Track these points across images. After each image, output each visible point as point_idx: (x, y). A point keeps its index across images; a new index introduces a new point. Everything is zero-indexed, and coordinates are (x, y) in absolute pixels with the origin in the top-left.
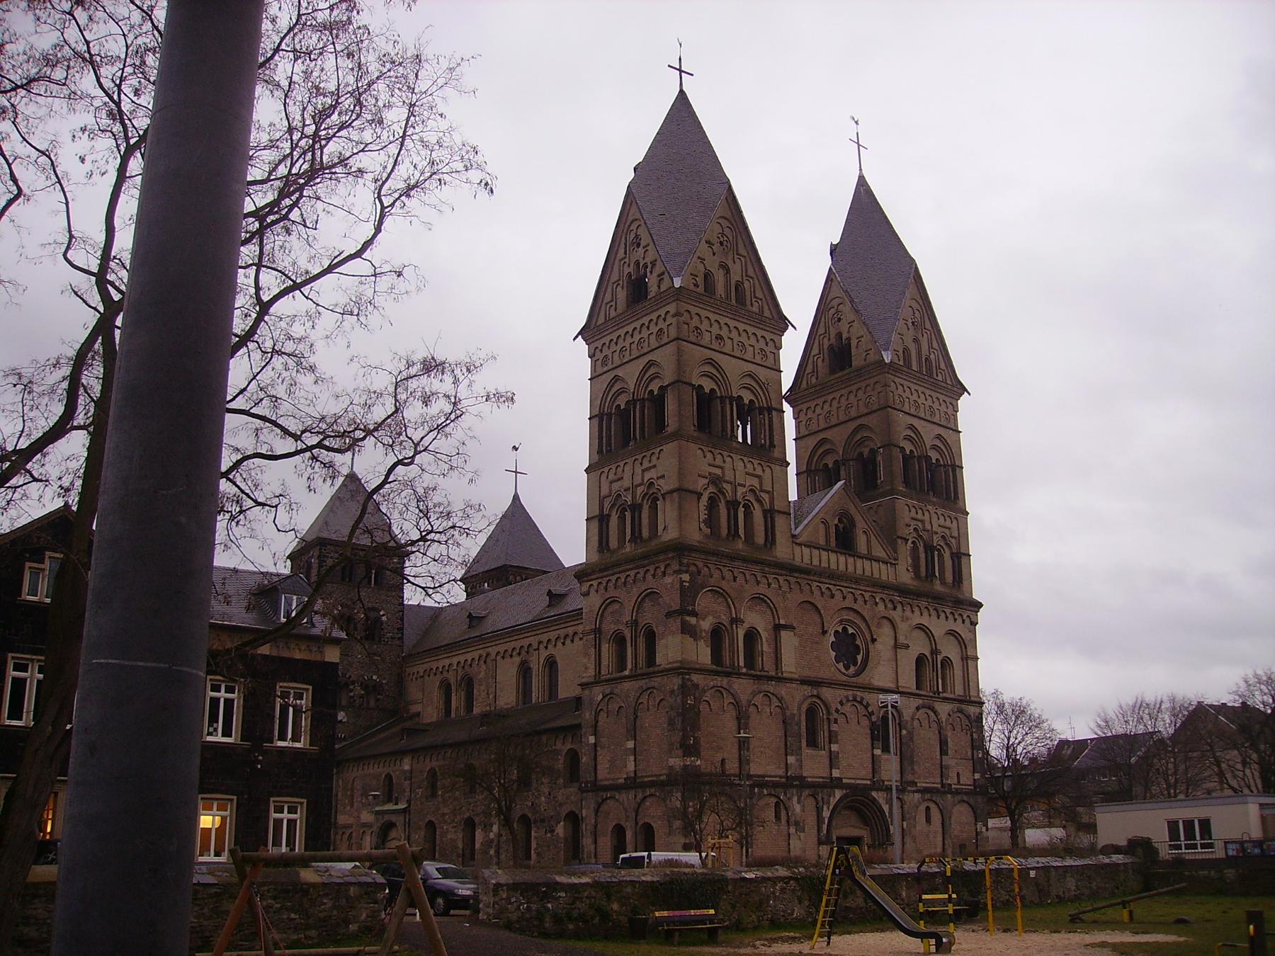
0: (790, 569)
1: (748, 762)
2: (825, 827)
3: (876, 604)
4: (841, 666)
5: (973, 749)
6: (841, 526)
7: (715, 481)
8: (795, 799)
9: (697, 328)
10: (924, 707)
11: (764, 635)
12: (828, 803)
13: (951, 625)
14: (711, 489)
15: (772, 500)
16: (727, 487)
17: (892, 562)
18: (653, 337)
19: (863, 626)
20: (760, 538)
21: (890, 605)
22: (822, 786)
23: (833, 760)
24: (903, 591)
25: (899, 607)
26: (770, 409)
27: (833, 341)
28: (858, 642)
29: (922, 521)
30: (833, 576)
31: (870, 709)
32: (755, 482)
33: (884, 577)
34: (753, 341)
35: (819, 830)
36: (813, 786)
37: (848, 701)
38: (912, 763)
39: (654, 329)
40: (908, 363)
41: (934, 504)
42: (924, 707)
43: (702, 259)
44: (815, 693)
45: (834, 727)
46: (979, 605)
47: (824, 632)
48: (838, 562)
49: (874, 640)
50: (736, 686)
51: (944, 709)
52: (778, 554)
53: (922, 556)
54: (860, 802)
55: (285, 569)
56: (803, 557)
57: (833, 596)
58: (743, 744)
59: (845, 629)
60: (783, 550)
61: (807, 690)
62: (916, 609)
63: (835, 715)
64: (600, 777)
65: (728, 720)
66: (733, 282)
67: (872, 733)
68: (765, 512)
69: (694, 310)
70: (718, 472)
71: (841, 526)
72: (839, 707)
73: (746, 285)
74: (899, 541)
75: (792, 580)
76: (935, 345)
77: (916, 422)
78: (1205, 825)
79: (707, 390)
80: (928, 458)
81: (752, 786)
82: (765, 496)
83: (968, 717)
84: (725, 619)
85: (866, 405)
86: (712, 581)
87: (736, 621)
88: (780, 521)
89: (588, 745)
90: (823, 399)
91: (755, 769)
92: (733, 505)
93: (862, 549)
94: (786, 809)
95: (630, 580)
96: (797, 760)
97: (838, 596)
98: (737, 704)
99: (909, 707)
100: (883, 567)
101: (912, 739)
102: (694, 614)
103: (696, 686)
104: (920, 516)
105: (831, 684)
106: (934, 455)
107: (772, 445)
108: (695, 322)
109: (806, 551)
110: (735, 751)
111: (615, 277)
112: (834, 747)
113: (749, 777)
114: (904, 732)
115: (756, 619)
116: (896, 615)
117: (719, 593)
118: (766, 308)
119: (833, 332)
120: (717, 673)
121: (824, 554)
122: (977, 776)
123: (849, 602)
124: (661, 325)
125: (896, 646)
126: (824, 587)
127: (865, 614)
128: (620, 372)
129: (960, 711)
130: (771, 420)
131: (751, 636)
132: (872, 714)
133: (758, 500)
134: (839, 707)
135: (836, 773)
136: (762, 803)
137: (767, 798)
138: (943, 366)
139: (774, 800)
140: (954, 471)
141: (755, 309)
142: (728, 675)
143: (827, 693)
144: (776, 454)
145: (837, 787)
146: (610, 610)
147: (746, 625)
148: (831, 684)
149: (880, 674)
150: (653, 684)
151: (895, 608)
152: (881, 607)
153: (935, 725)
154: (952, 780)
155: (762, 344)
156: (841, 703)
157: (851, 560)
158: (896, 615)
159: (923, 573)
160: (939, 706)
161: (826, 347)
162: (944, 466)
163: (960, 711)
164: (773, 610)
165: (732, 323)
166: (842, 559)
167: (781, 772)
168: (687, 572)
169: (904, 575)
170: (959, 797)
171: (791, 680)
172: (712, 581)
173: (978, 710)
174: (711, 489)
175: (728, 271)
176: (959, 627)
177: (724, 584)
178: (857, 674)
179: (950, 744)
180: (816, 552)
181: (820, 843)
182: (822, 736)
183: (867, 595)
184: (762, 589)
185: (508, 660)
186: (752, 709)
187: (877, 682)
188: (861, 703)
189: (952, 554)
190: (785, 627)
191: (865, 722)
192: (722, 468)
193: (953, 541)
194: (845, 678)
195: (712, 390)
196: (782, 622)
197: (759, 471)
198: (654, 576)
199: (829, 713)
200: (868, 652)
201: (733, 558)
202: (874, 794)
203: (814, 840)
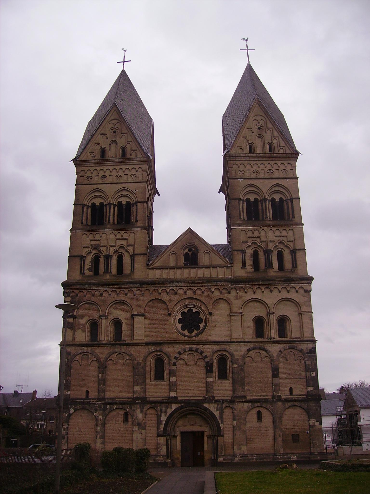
0: (141, 283)
1: (104, 391)
2: (162, 426)
3: (212, 292)
4: (186, 332)
5: (306, 370)
6: (190, 253)
7: (96, 247)
8: (138, 410)
9: (89, 177)
12: (166, 412)
13: (285, 294)
14: (94, 252)
16: (104, 249)
17: (230, 265)
19: (202, 307)
21: (224, 291)
22: (161, 402)
23: (172, 387)
24: (237, 282)
25: (233, 292)
28: (201, 316)
30: (173, 282)
31: (204, 355)
32: (124, 243)
34: (127, 172)
35: (158, 427)
36: (154, 404)
37: (185, 351)
38: (243, 384)
41: (269, 225)
42: (254, 349)
43: (98, 144)
44: (158, 349)
45: (174, 368)
46: (312, 279)
48: (186, 273)
50: (97, 351)
51: (274, 350)
52: (136, 277)
54: (192, 408)
57: (176, 293)
58: (102, 382)
59: (190, 310)
60: (139, 274)
61: (152, 348)
63: (174, 361)
65: (93, 369)
67: (207, 369)
69: (86, 169)
71: (190, 253)
72: (178, 356)
75: (144, 289)
76: (276, 134)
77: (253, 182)
81: (105, 404)
82: (131, 249)
83: (301, 351)
84: (96, 316)
86: (85, 298)
91: (108, 395)
92: (108, 257)
94: (132, 416)
96: (142, 388)
97: (180, 293)
98: (98, 360)
99: (238, 351)
101: (243, 370)
102: (74, 317)
103: (69, 354)
105: (170, 343)
108: (89, 173)
109: (158, 272)
110: (96, 386)
112: (173, 379)
113: (104, 399)
115: (121, 314)
117: (91, 304)
118: (139, 153)
122: (310, 389)
123: (190, 294)
125: (231, 315)
126: (168, 289)
127: (203, 299)
131: (117, 324)
132: (206, 357)
134: (178, 356)
135: (173, 394)
136: (112, 414)
137: (118, 411)
138: (282, 144)
139: (122, 412)
140: (292, 202)
143: (167, 349)
145: (173, 403)
147: (110, 318)
148: (170, 343)
151: (229, 292)
152: (217, 293)
153: (267, 360)
154: (284, 393)
155: (134, 172)
156: (180, 353)
158: (231, 296)
160: (269, 347)
162: (286, 201)
163: (294, 348)
164: (130, 307)
165: (111, 168)
167: (130, 396)
168: (69, 296)
169: (239, 272)
170: (290, 404)
171: (138, 344)
172: (85, 298)
173: (310, 346)
174: (94, 252)
176: (292, 295)
177: (93, 299)
179: (282, 369)
181: (159, 435)
182: (166, 373)
184: (122, 297)
187: (213, 338)
188: (196, 351)
189: (291, 251)
190: (137, 315)
191: (202, 363)
193: (291, 244)
196: (135, 313)
197: (125, 236)
199: (169, 360)
201: (106, 284)
202: (206, 405)
203: (155, 434)
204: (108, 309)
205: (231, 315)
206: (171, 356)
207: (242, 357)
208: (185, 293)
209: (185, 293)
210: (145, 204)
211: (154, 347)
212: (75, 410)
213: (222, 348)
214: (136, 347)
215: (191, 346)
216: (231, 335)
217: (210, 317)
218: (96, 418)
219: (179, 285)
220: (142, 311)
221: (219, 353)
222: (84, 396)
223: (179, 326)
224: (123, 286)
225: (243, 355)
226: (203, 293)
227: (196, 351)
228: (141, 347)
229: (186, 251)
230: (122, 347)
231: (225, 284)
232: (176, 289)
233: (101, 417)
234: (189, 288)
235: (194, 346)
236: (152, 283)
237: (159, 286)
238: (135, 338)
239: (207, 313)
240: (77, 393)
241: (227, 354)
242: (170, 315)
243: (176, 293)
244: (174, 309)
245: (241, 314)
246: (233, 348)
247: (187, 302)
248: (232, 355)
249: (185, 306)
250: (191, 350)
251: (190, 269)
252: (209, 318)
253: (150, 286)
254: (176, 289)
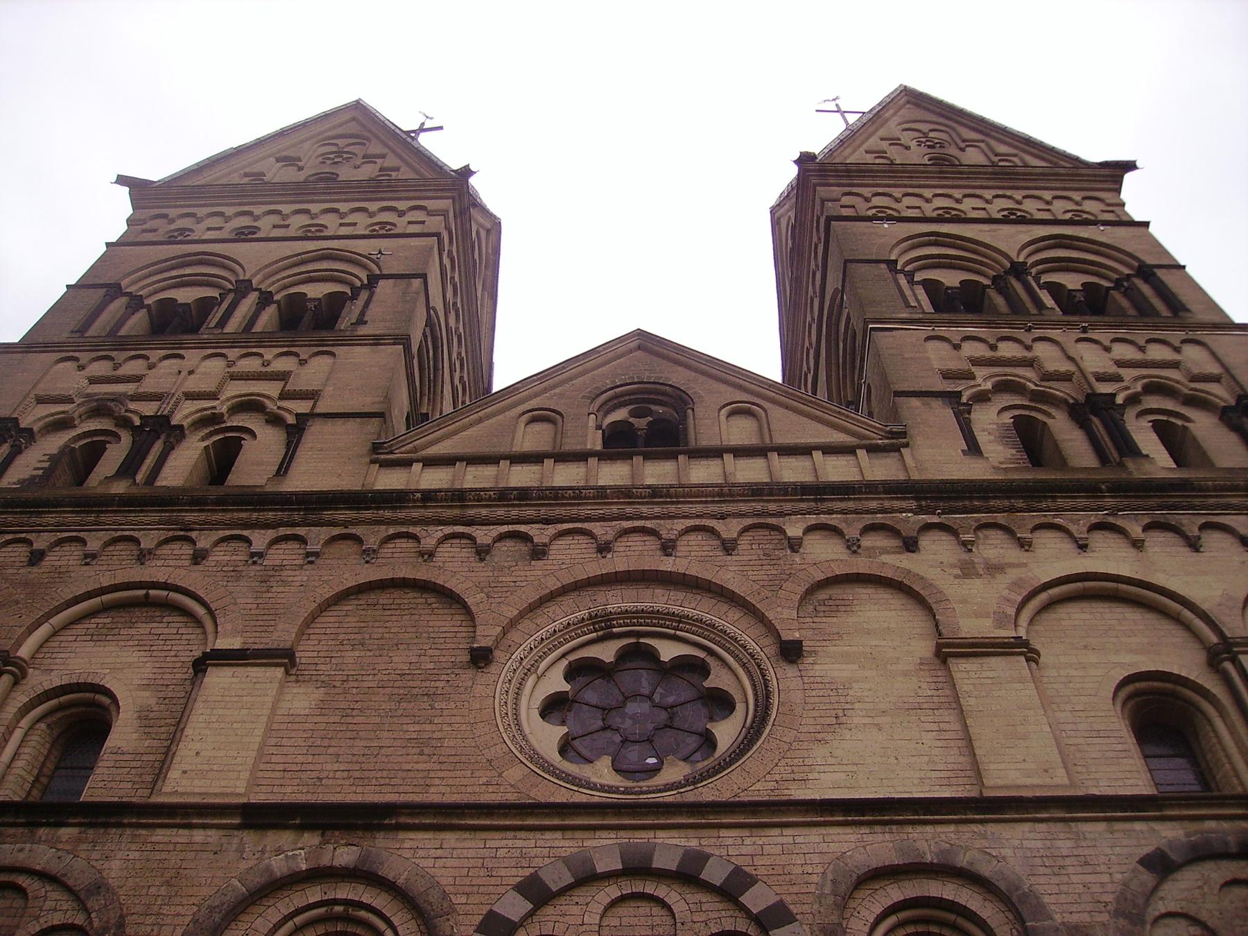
3: (795, 545)
24: (944, 499)
28: (718, 679)
37: (587, 878)
44: (344, 855)
49: (791, 652)
61: (291, 851)
126: (483, 535)
147: (39, 681)
188: (688, 875)
196: (222, 644)
197: (281, 365)
204: (45, 629)
205: (949, 650)
206: (452, 910)
207: (1117, 913)
209: (604, 548)
210: (417, 283)
211: (311, 839)
213: (922, 846)
214: (160, 835)
215: (642, 837)
217: (790, 671)
219: (560, 511)
220: (282, 635)
221: (895, 893)
223: (547, 737)
225: (1122, 897)
226: (729, 547)
227: (688, 875)
228: (199, 836)
229: (620, 415)
230: (42, 832)
231: (873, 504)
232: (541, 534)
234: (627, 524)
239: (762, 648)
242: (481, 658)
243: (539, 553)
244: (514, 636)
245: (1022, 648)
246: (1010, 848)
247: (616, 601)
249: (603, 626)
251: (637, 460)
252: (784, 679)
253: (367, 514)
254: (541, 534)
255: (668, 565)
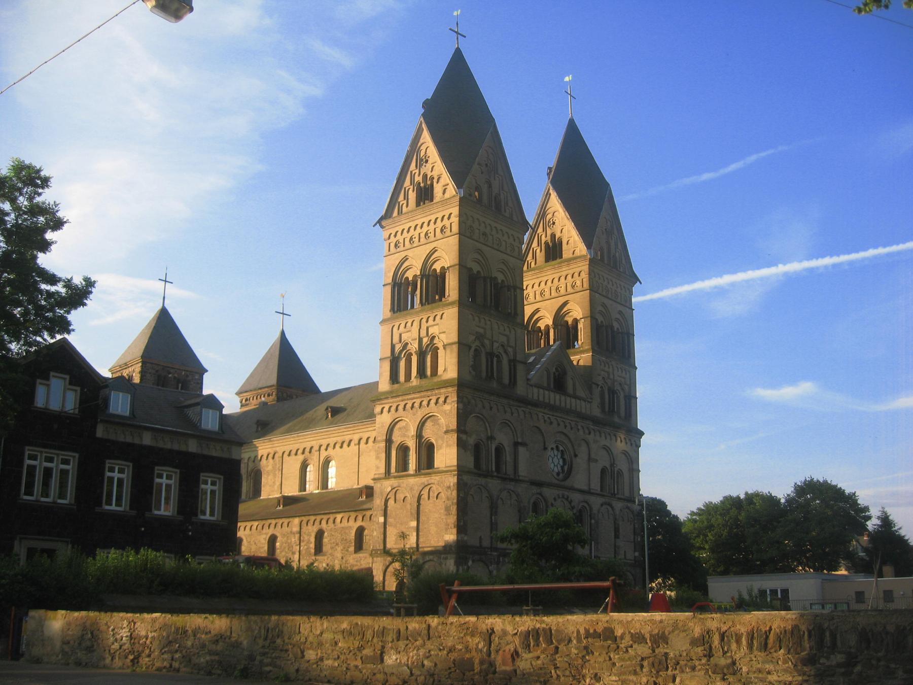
5: (635, 534)
9: (471, 227)
10: (605, 503)
11: (507, 449)
14: (477, 343)
15: (515, 353)
16: (487, 342)
18: (438, 231)
20: (506, 381)
21: (587, 432)
24: (596, 421)
25: (592, 432)
26: (515, 288)
27: (549, 237)
28: (565, 457)
29: (608, 372)
30: (553, 408)
31: (573, 504)
33: (583, 411)
39: (439, 224)
40: (602, 259)
44: (539, 491)
46: (641, 434)
47: (545, 449)
48: (554, 398)
49: (576, 456)
51: (618, 505)
52: (519, 392)
53: (607, 396)
55: (206, 392)
56: (535, 394)
57: (551, 423)
61: (535, 489)
62: (603, 435)
64: (388, 546)
66: (494, 194)
68: (510, 361)
70: (481, 331)
73: (502, 197)
74: (594, 386)
77: (606, 301)
78: (785, 592)
79: (475, 272)
80: (612, 327)
82: (510, 350)
83: (633, 512)
85: (573, 287)
87: (491, 438)
88: (520, 368)
89: (378, 523)
90: (540, 280)
92: (491, 355)
93: (570, 390)
95: (417, 405)
99: (596, 502)
100: (583, 403)
104: (606, 369)
105: (550, 485)
106: (616, 325)
107: (516, 314)
109: (535, 390)
111: (407, 183)
114: (593, 521)
115: (503, 438)
116: (590, 438)
119: (549, 232)
120: (480, 475)
121: (547, 392)
124: (446, 222)
125: (590, 459)
126: (546, 417)
128: (410, 253)
129: (628, 508)
130: (515, 296)
131: (499, 450)
132: (573, 508)
133: (506, 352)
140: (628, 337)
141: (507, 214)
142: (485, 476)
143: (547, 492)
144: (519, 320)
146: (397, 426)
148: (550, 485)
149: (579, 480)
150: (433, 481)
151: (590, 433)
152: (581, 432)
156: (555, 499)
157: (563, 398)
158: (590, 438)
159: (607, 409)
161: (543, 242)
166: (558, 397)
171: (523, 481)
174: (477, 343)
175: (490, 186)
178: (565, 479)
180: (541, 391)
183: (573, 424)
185: (293, 457)
186: (500, 501)
187: (577, 486)
188: (567, 499)
192: (485, 329)
194: (556, 482)
195: (478, 272)
196: (520, 440)
197: (507, 332)
198: (436, 403)
199: (547, 506)
200: (572, 462)
208: (559, 425)
212: (473, 561)
216: (589, 485)
218: (491, 572)
222: (478, 545)
224: (512, 402)
232: (552, 418)
233: (495, 572)
235: (566, 493)
236: (536, 404)
237: (542, 410)
238: (521, 473)
240: (473, 541)
241: (586, 505)
248: (591, 509)
250: (563, 497)
254: (552, 418)
255: (565, 431)
